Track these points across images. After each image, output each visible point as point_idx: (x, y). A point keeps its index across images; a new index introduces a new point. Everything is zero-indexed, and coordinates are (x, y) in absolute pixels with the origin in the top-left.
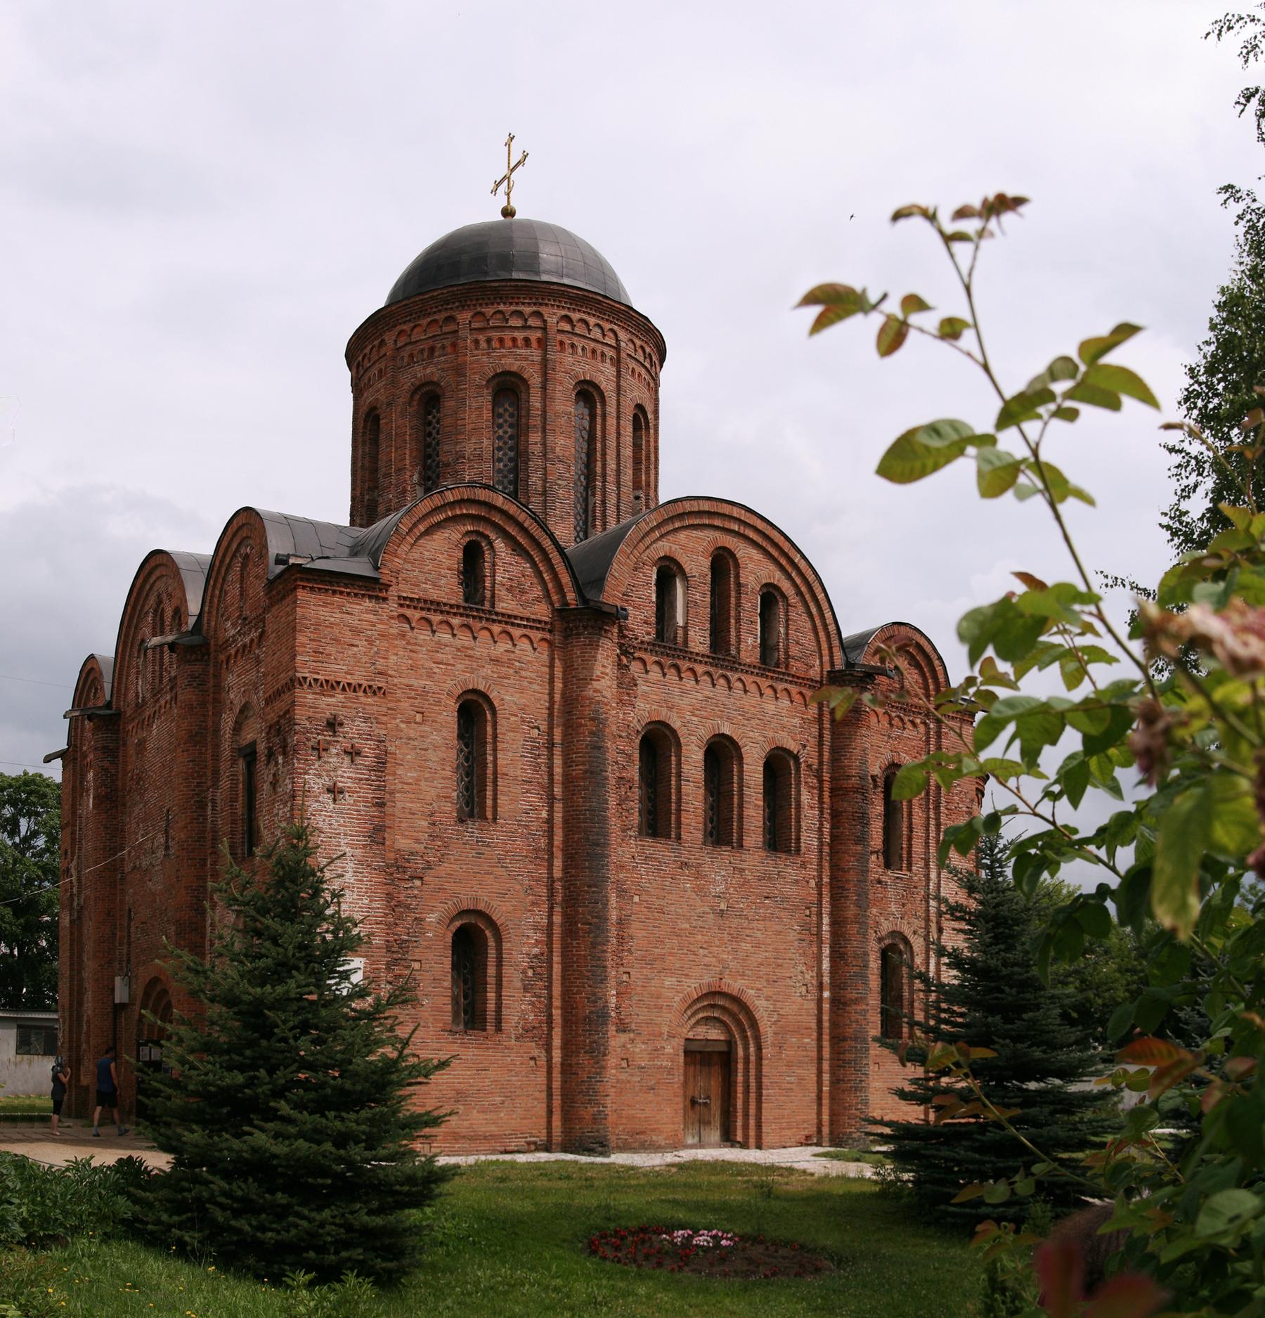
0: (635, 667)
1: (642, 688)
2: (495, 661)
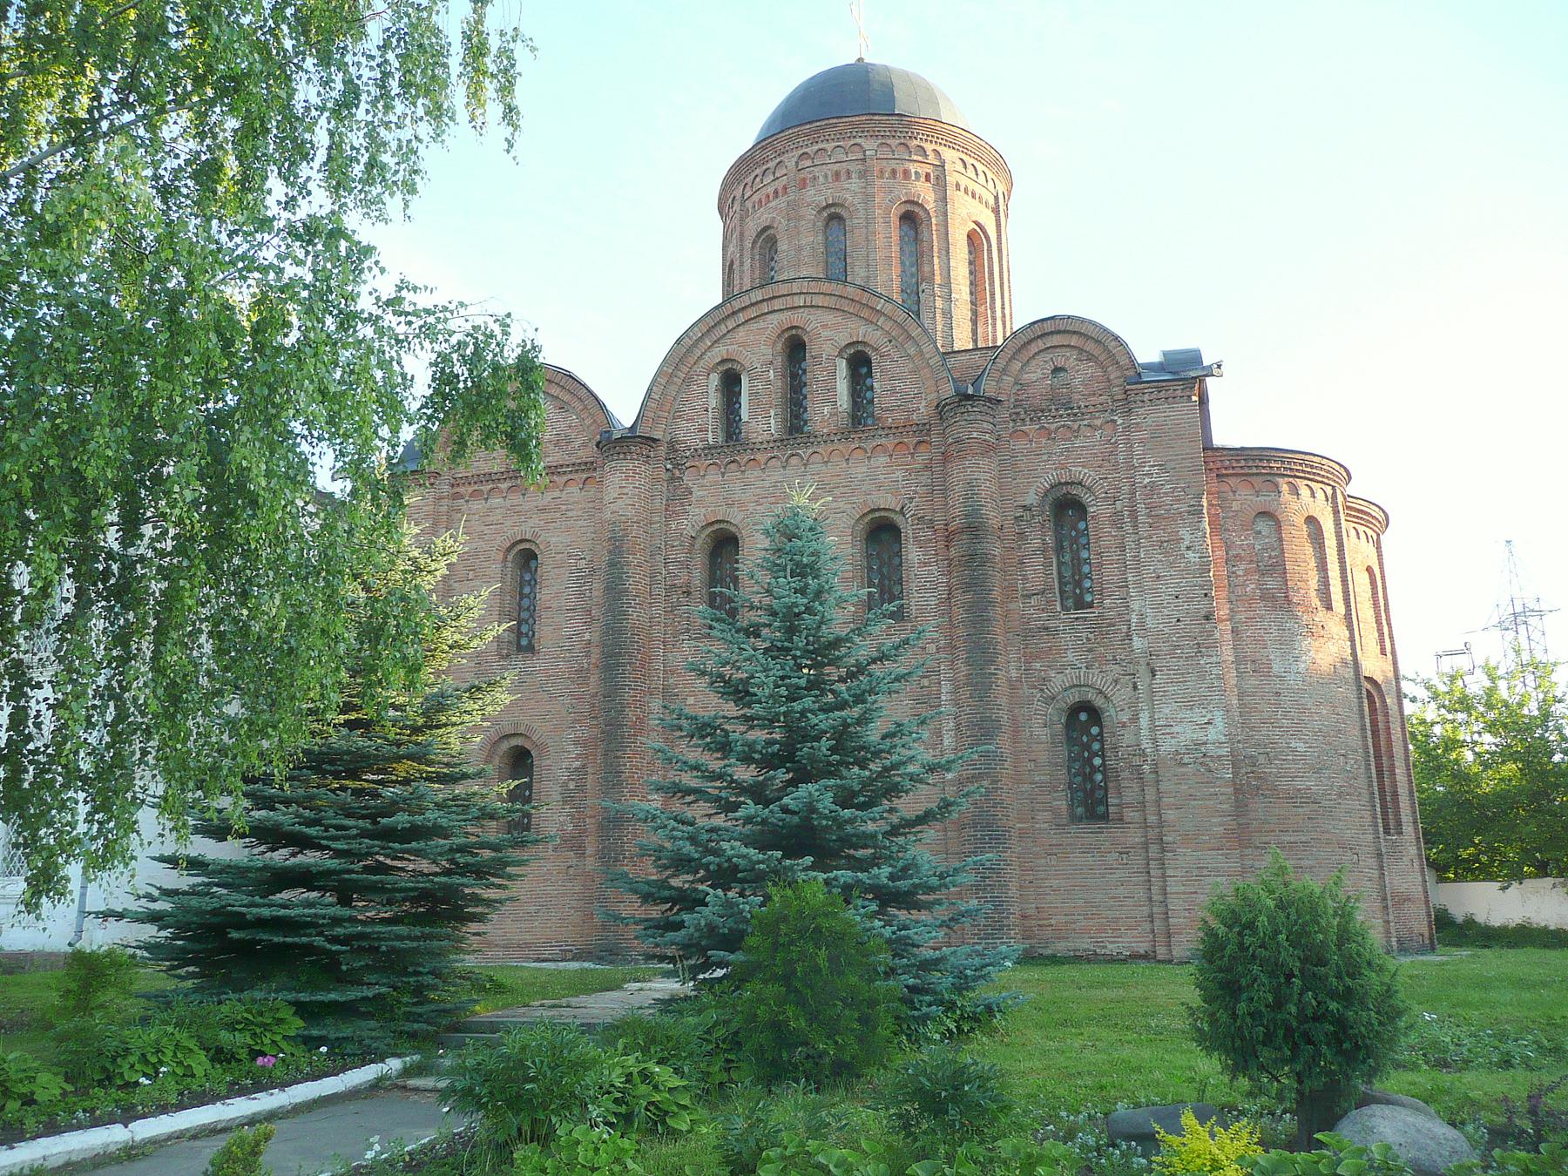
0: (688, 478)
1: (697, 493)
2: (543, 510)
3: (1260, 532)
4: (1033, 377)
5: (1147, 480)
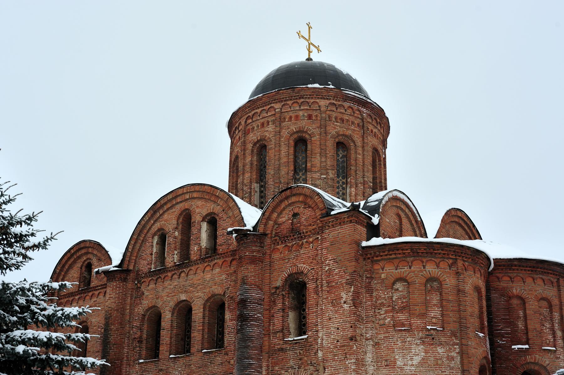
3: (398, 290)
4: (284, 219)
5: (327, 268)
